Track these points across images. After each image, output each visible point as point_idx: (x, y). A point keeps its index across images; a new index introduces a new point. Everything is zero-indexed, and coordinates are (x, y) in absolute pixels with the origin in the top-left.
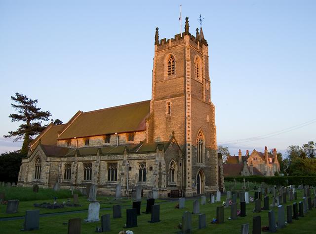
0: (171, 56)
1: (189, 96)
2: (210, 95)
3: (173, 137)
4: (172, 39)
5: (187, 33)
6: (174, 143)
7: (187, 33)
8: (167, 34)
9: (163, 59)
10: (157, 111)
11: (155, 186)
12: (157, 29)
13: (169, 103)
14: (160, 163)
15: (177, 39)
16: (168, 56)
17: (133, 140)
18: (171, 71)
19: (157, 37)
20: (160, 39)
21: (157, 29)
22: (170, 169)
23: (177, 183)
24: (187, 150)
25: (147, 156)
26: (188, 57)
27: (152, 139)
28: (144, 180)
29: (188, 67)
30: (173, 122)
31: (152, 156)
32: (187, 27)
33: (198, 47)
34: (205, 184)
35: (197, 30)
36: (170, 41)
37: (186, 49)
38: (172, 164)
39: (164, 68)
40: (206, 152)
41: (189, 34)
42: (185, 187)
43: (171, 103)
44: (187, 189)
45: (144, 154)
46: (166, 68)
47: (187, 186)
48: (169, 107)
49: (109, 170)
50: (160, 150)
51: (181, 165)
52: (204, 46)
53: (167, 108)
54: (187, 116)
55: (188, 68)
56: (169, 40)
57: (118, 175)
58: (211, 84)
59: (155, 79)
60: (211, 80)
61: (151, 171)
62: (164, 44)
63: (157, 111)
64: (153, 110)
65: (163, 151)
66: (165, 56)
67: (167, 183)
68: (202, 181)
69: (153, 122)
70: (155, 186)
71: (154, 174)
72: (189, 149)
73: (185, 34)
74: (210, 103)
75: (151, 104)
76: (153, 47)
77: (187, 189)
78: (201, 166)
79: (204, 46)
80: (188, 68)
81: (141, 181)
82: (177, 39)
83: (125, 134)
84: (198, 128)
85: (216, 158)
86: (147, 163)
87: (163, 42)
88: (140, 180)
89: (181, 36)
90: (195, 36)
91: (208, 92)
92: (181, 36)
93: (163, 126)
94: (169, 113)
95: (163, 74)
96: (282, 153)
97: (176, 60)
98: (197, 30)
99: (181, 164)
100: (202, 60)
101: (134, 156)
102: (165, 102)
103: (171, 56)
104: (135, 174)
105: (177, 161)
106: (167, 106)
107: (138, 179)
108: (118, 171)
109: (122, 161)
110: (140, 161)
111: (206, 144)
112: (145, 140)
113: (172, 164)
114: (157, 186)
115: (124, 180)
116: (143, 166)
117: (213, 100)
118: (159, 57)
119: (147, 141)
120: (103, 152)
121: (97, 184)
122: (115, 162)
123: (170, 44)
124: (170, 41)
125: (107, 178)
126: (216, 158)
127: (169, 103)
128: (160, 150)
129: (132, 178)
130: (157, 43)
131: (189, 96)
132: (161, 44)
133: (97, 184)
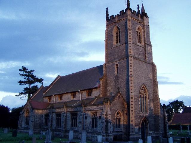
0: (118, 28)
1: (131, 58)
2: (152, 56)
3: (119, 92)
4: (118, 15)
5: (128, 9)
6: (119, 97)
7: (128, 9)
8: (114, 12)
9: (112, 30)
10: (108, 72)
11: (102, 132)
12: (107, 9)
13: (117, 65)
14: (107, 113)
15: (121, 14)
16: (115, 28)
17: (91, 96)
18: (118, 40)
19: (107, 14)
20: (109, 16)
21: (107, 9)
22: (116, 118)
23: (123, 129)
24: (130, 102)
25: (97, 107)
26: (129, 28)
27: (106, 95)
28: (96, 127)
29: (130, 35)
30: (120, 80)
31: (101, 108)
32: (128, 4)
33: (140, 19)
34: (149, 130)
35: (138, 6)
36: (116, 17)
37: (128, 21)
38: (118, 114)
39: (113, 37)
40: (150, 103)
41: (131, 10)
42: (129, 132)
43: (118, 65)
44: (130, 134)
45: (95, 107)
46: (114, 37)
47: (131, 132)
48: (117, 68)
49: (72, 118)
50: (105, 102)
51: (126, 115)
52: (145, 18)
53: (116, 69)
54: (130, 74)
55: (129, 36)
56: (115, 16)
57: (78, 123)
58: (153, 48)
59: (107, 47)
60: (152, 44)
61: (100, 120)
62: (113, 19)
63: (108, 72)
64: (106, 72)
65: (109, 103)
66: (113, 28)
67: (113, 129)
68: (146, 128)
69: (106, 80)
70: (102, 132)
71: (102, 122)
72: (132, 101)
73: (126, 10)
74: (153, 63)
75: (104, 67)
76: (105, 23)
77: (130, 134)
78: (145, 115)
79: (145, 18)
80: (129, 36)
81: (93, 127)
82: (121, 14)
83: (85, 91)
84: (141, 84)
85: (158, 108)
86: (97, 113)
87: (111, 18)
88: (93, 127)
89: (124, 12)
90: (137, 11)
91: (151, 54)
92: (124, 12)
93: (113, 84)
94: (117, 73)
95: (112, 43)
96: (183, 101)
97: (121, 31)
98: (138, 6)
99: (126, 113)
100: (144, 28)
101: (88, 107)
102: (114, 64)
103: (118, 28)
104: (89, 122)
105: (123, 111)
106: (116, 67)
107: (91, 125)
108: (78, 119)
109: (80, 112)
110: (92, 112)
111: (149, 97)
112: (99, 95)
113: (118, 114)
114: (104, 132)
115: (81, 127)
116: (95, 116)
117: (155, 61)
118: (109, 29)
119: (101, 96)
120: (68, 105)
121: (64, 130)
122: (76, 113)
123: (117, 19)
124: (116, 17)
125: (71, 125)
126: (158, 108)
127: (117, 65)
128: (105, 102)
129: (87, 126)
130: (107, 19)
131: (131, 58)
132: (110, 20)
133: (64, 130)
